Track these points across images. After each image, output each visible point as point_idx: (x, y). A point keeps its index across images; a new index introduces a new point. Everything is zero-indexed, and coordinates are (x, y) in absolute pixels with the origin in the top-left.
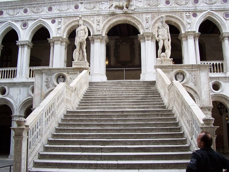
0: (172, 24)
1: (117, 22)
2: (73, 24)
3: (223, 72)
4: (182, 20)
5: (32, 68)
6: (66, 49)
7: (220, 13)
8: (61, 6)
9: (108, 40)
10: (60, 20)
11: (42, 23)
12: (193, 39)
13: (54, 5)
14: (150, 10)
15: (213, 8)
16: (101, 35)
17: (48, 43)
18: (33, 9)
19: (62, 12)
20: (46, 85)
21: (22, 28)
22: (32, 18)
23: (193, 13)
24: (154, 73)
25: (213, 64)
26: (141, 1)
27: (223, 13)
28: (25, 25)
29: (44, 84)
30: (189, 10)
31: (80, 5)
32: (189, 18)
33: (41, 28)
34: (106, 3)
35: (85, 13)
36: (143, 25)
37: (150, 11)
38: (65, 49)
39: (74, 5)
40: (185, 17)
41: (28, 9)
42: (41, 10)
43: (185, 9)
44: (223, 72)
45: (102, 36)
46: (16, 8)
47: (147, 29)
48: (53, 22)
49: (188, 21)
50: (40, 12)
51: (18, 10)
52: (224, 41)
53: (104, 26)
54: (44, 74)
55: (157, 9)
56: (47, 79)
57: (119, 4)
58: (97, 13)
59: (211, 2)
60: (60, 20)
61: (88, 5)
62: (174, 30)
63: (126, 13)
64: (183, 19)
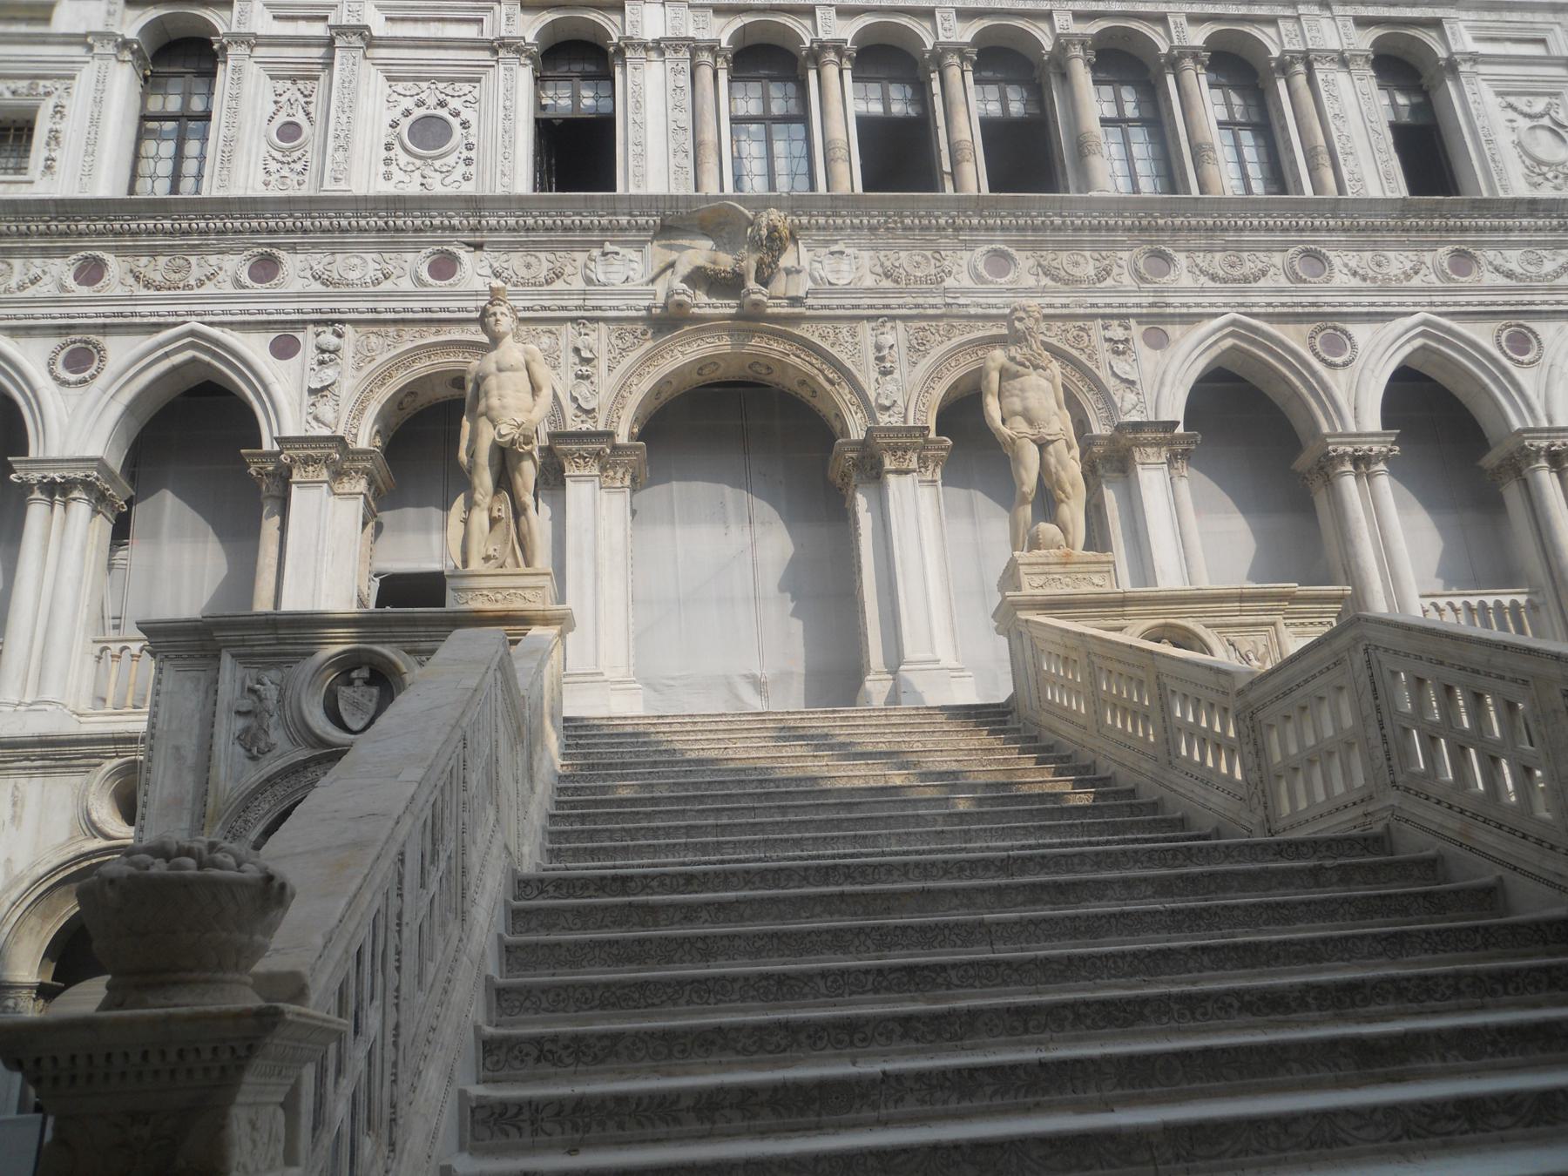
1: (702, 364)
7: (1291, 328)
8: (338, 257)
10: (328, 339)
11: (207, 351)
13: (293, 248)
14: (901, 301)
15: (1254, 300)
18: (144, 260)
19: (343, 289)
21: (56, 378)
22: (133, 314)
26: (842, 253)
27: (1307, 328)
28: (81, 359)
30: (1124, 310)
31: (464, 255)
32: (1124, 353)
34: (630, 253)
36: (866, 387)
37: (900, 306)
40: (1104, 353)
41: (108, 257)
42: (196, 273)
43: (1100, 301)
46: (28, 253)
47: (888, 408)
48: (284, 349)
49: (1122, 367)
50: (193, 282)
51: (38, 262)
53: (625, 386)
54: (226, 660)
55: (938, 301)
57: (714, 263)
59: (1237, 273)
60: (328, 339)
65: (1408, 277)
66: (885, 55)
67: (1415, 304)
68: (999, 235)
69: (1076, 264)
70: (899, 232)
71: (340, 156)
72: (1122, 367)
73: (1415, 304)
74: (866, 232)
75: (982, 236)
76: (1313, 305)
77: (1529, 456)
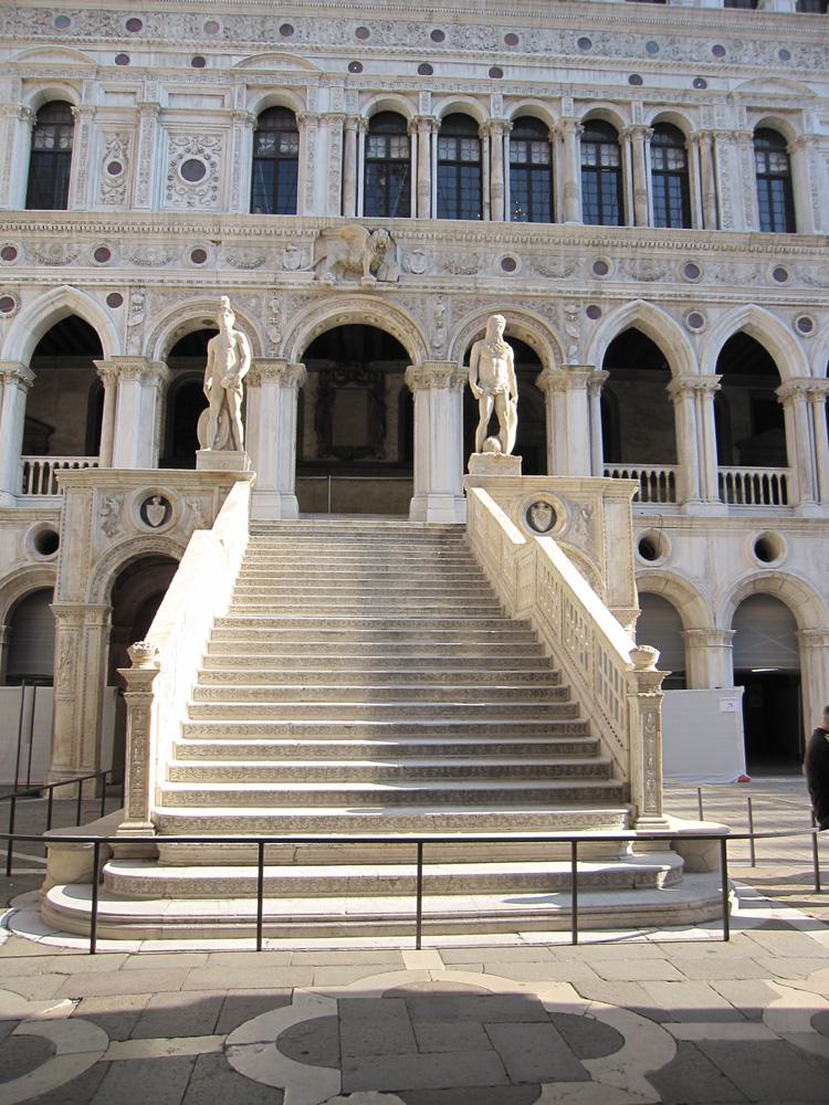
0: (519, 337)
1: (338, 317)
2: (185, 314)
3: (673, 499)
4: (551, 328)
5: (32, 460)
6: (160, 400)
7: (673, 309)
9: (304, 377)
12: (585, 391)
14: (451, 285)
16: (285, 360)
17: (96, 375)
20: (105, 527)
22: (34, 279)
23: (588, 305)
24: (456, 497)
25: (644, 473)
29: (96, 523)
33: (63, 321)
35: (230, 280)
37: (450, 288)
38: (157, 399)
39: (190, 246)
40: (562, 316)
44: (673, 499)
45: (288, 366)
48: (114, 301)
49: (572, 330)
50: (64, 260)
52: (681, 401)
56: (108, 505)
58: (272, 284)
59: (647, 274)
60: (137, 298)
61: (241, 252)
62: (528, 361)
63: (370, 291)
64: (555, 323)
65: (749, 281)
66: (459, 124)
67: (748, 298)
68: (512, 246)
69: (555, 264)
70: (454, 242)
71: (143, 186)
72: (572, 330)
73: (748, 298)
74: (435, 242)
75: (501, 245)
76: (688, 296)
77: (795, 391)
